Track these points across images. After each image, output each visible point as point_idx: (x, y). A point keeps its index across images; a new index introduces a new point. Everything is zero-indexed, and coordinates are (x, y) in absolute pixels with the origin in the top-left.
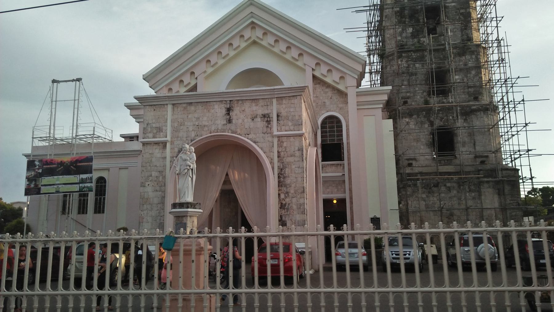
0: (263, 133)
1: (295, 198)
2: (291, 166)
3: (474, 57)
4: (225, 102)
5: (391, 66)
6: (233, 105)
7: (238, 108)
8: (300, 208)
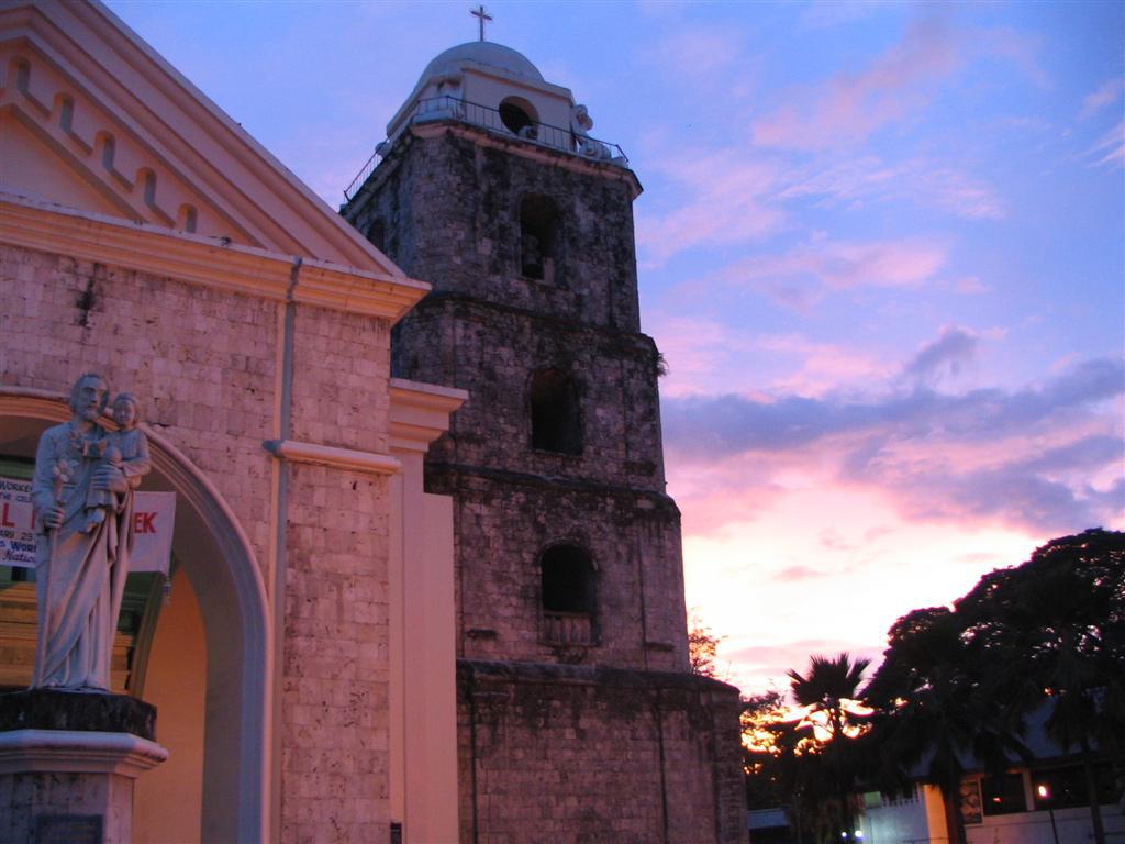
0: (228, 433)
1: (352, 729)
2: (340, 588)
3: (641, 368)
4: (65, 263)
5: (428, 336)
6: (107, 287)
7: (129, 304)
8: (371, 772)
